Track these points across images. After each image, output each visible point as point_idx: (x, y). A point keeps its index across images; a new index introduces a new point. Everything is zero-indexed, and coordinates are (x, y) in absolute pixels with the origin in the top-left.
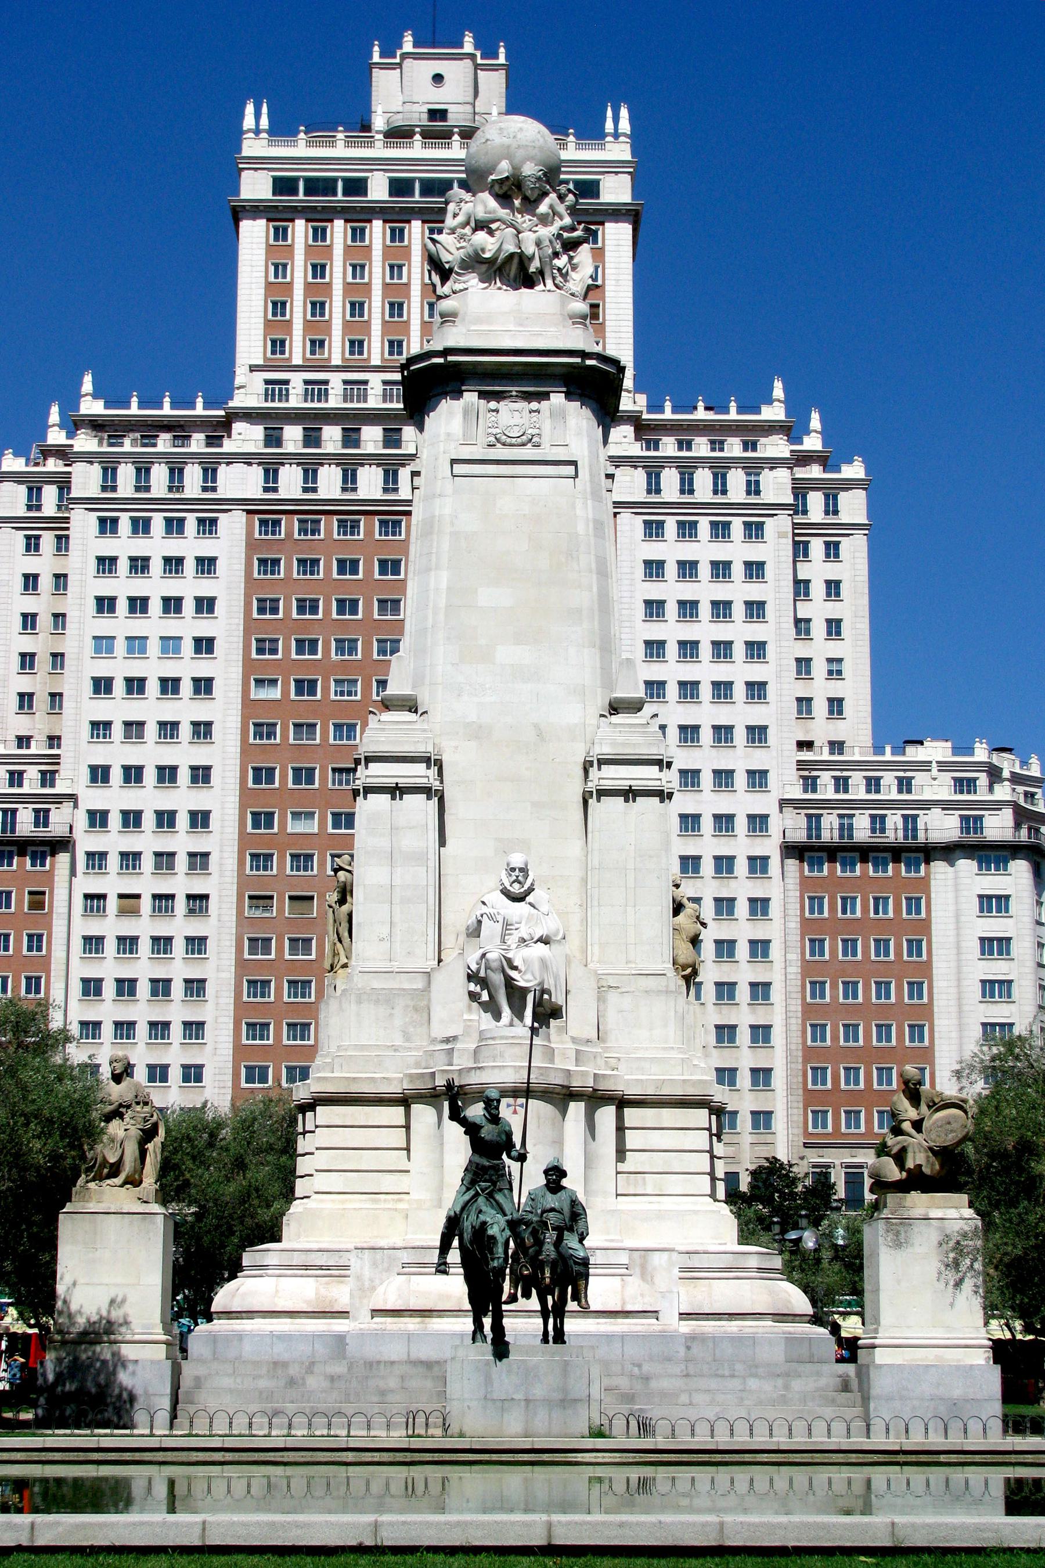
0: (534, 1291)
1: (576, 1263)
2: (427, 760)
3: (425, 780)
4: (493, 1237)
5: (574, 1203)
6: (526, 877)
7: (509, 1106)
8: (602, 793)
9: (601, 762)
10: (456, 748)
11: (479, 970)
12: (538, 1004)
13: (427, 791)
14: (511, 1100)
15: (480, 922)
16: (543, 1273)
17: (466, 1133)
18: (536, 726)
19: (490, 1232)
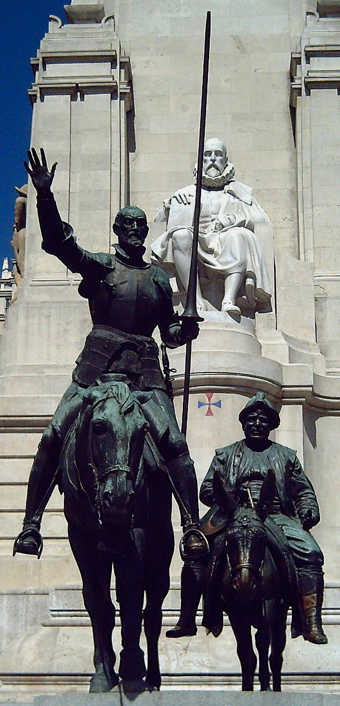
0: (226, 618)
1: (300, 563)
2: (113, 60)
3: (111, 79)
4: (104, 427)
5: (292, 467)
6: (225, 162)
7: (200, 404)
8: (310, 86)
9: (309, 55)
10: (147, 62)
11: (165, 254)
12: (241, 290)
13: (113, 91)
14: (204, 397)
15: (167, 210)
16: (236, 561)
17: (83, 290)
18: (236, 39)
19: (97, 416)
